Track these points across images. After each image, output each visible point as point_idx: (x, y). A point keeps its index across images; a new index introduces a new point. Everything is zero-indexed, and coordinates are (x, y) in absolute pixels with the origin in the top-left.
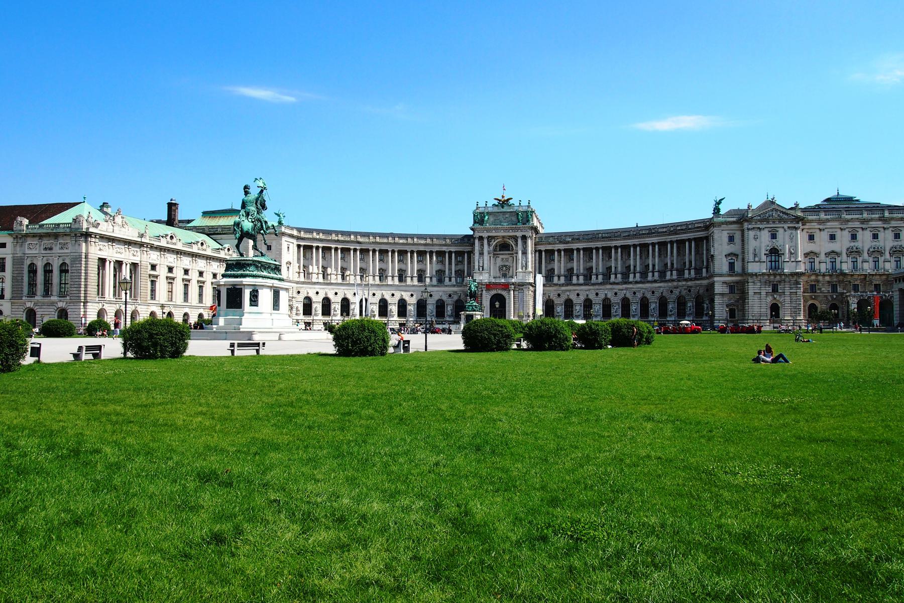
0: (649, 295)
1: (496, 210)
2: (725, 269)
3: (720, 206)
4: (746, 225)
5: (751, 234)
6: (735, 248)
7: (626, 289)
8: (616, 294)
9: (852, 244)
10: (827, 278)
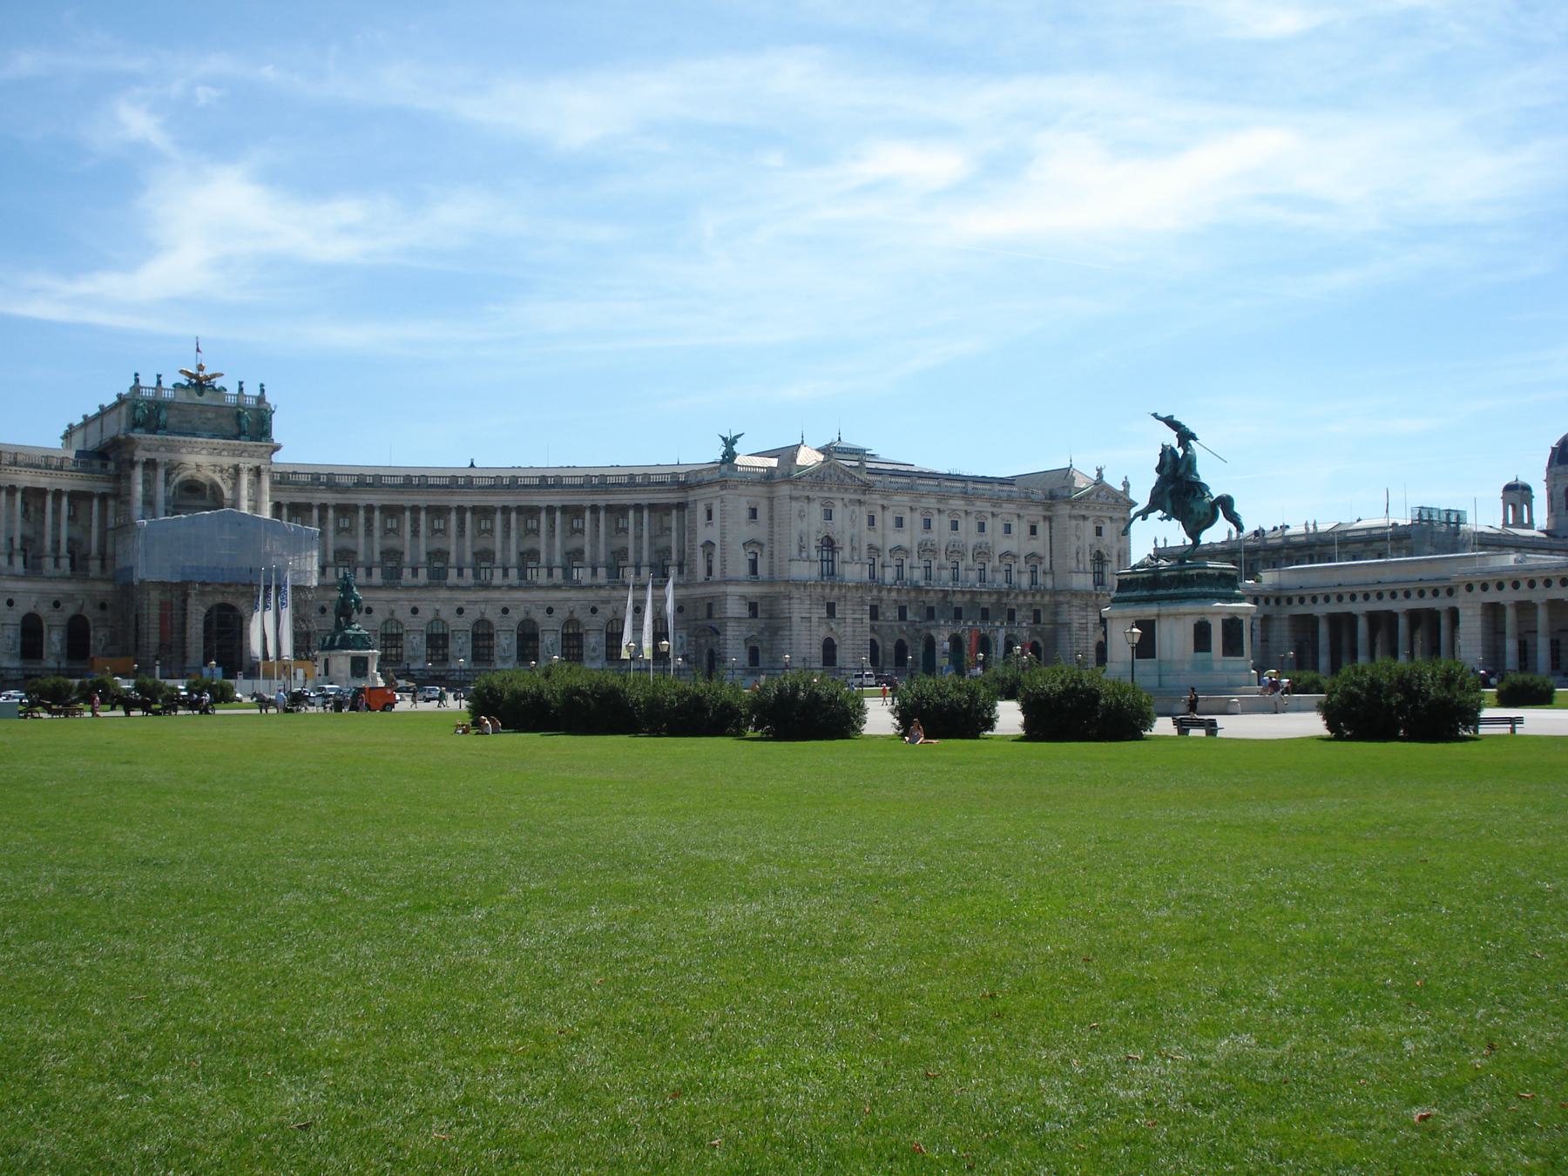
0: (539, 616)
1: (182, 397)
2: (743, 570)
3: (736, 448)
4: (785, 490)
5: (796, 506)
6: (759, 531)
7: (487, 601)
8: (460, 611)
9: (926, 536)
10: (894, 595)
